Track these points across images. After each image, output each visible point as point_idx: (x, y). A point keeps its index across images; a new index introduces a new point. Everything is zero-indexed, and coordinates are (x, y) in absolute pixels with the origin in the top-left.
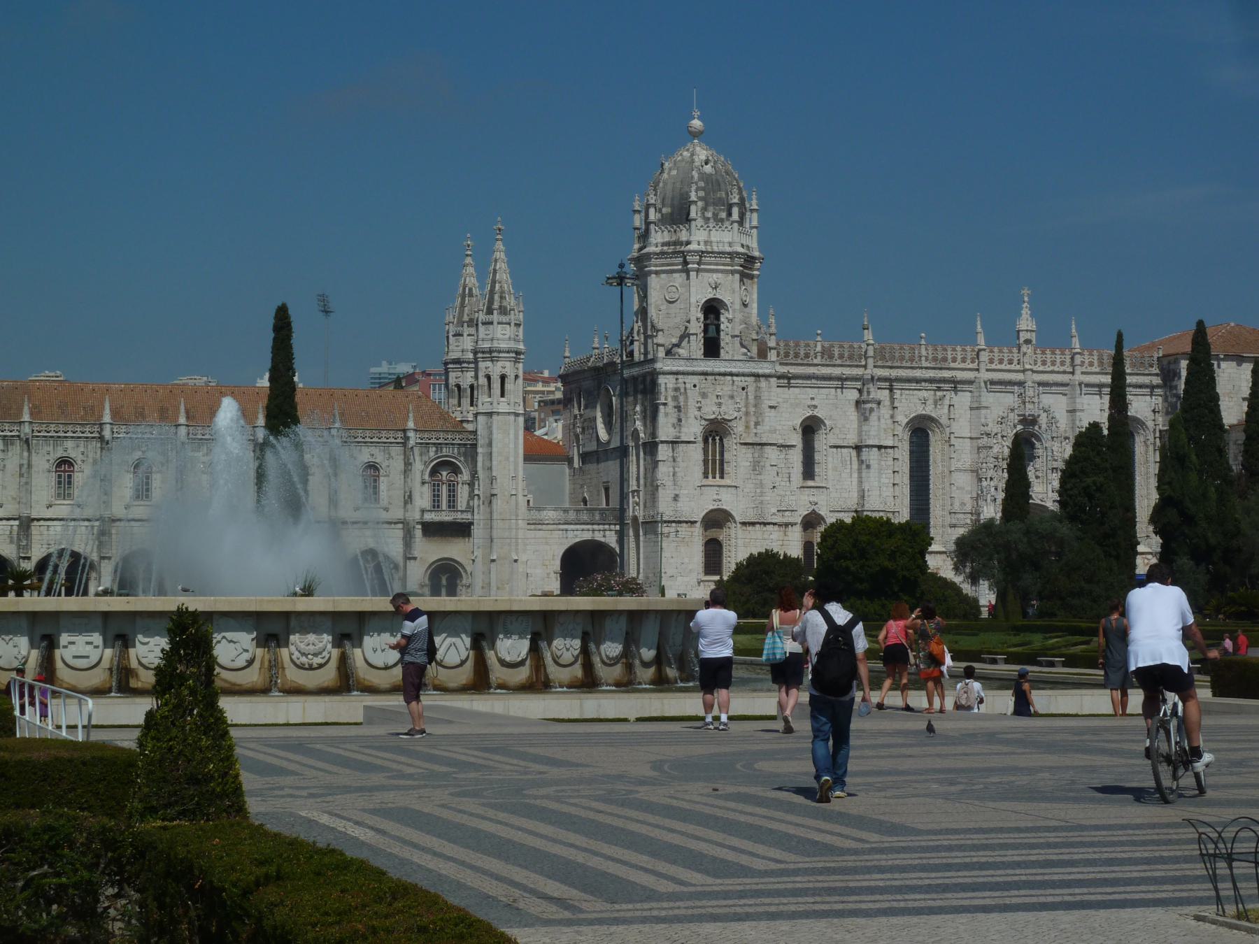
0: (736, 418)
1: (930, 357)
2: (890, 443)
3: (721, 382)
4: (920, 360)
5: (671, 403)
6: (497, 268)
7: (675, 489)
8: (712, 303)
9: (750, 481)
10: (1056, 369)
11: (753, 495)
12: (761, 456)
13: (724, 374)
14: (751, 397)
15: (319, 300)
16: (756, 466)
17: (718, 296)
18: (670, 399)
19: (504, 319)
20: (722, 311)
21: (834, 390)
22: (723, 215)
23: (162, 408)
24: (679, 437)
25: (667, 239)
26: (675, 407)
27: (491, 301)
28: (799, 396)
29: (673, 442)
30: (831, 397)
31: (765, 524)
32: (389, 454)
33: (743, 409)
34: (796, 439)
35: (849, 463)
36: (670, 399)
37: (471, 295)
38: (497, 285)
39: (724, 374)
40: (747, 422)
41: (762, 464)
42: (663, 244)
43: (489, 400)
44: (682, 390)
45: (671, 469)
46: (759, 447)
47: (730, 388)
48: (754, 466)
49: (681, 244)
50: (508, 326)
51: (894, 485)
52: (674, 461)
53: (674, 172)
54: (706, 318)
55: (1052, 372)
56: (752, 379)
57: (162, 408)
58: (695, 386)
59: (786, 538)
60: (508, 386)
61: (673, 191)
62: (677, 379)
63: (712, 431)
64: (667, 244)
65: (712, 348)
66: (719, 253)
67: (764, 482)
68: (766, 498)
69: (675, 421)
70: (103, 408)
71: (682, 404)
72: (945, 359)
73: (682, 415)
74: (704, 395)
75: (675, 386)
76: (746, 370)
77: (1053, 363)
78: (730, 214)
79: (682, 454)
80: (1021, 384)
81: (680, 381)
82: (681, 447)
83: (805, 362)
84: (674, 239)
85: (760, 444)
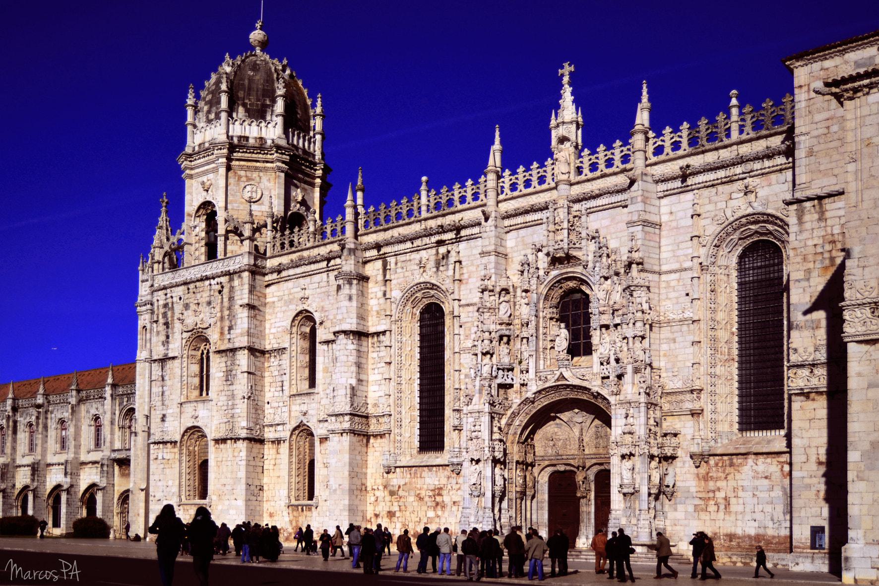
3: (201, 289)
5: (161, 321)
9: (223, 393)
11: (225, 408)
12: (233, 364)
16: (229, 377)
18: (160, 317)
28: (292, 291)
30: (322, 284)
31: (236, 439)
33: (219, 315)
36: (160, 317)
40: (222, 328)
41: (234, 372)
48: (227, 376)
52: (163, 380)
58: (180, 299)
59: (278, 456)
62: (166, 294)
67: (235, 392)
69: (163, 338)
75: (165, 302)
79: (168, 372)
81: (169, 296)
82: (169, 364)
83: (299, 248)
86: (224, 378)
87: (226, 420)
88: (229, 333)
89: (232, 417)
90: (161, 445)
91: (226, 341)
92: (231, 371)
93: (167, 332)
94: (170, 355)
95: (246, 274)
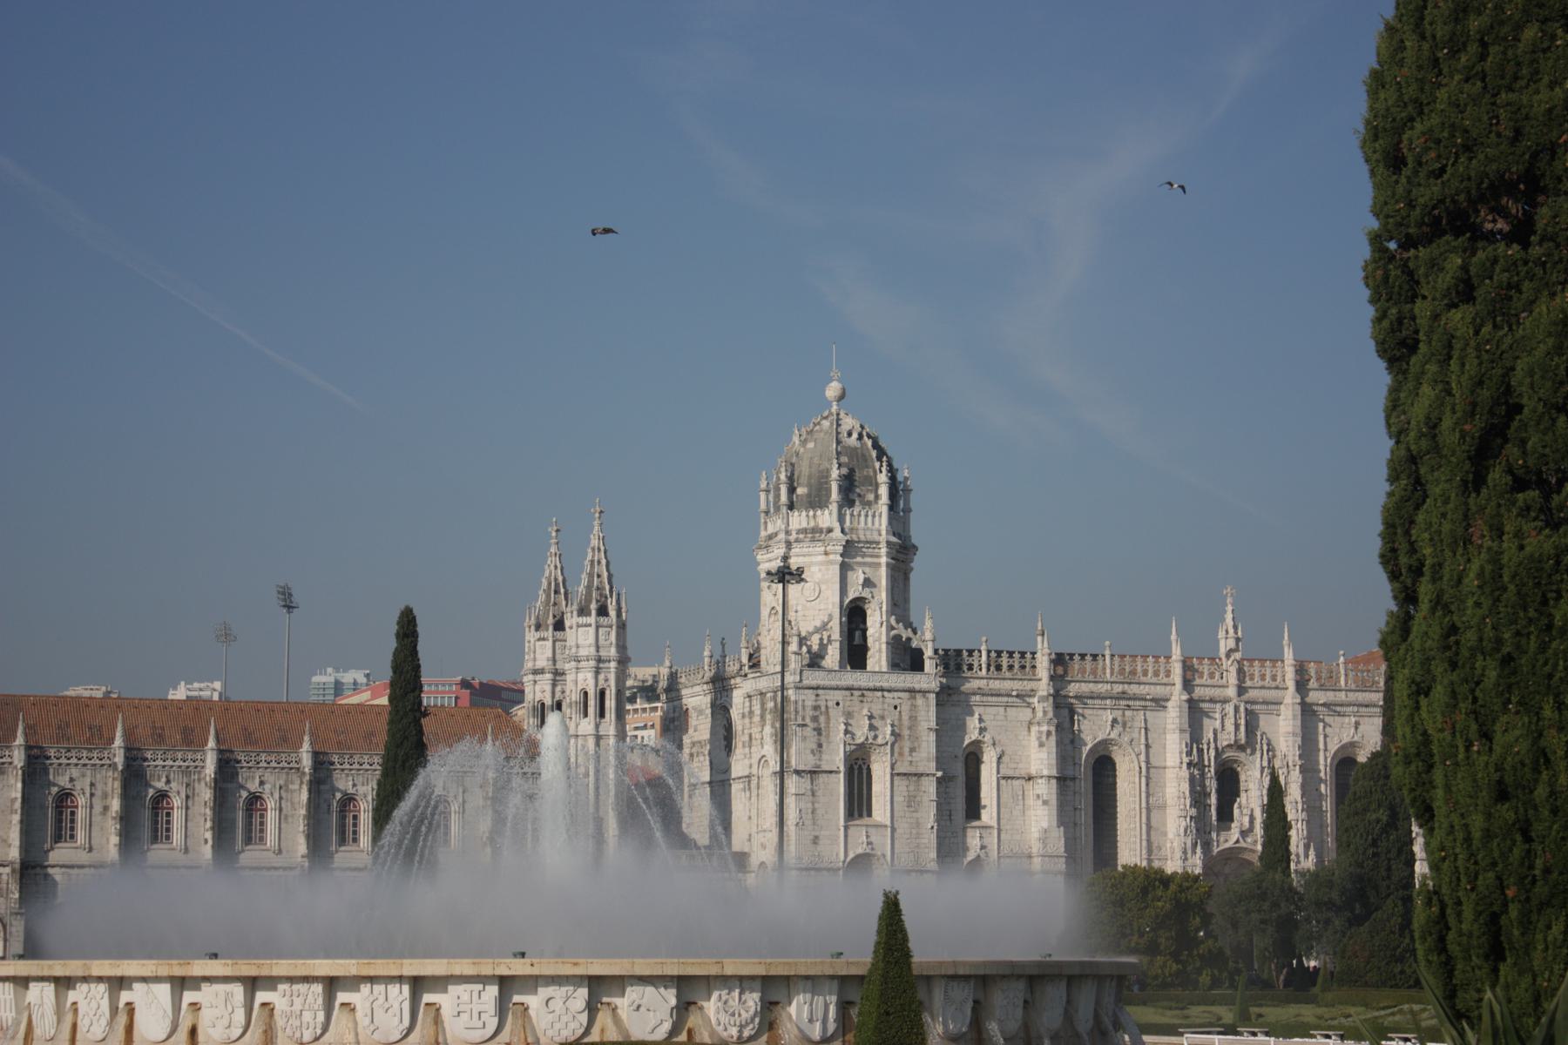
0: (887, 743)
1: (1116, 668)
2: (1070, 773)
3: (869, 700)
4: (1105, 674)
6: (596, 558)
7: (814, 830)
8: (858, 603)
10: (1266, 683)
11: (906, 836)
13: (875, 690)
14: (905, 717)
15: (279, 592)
16: (912, 802)
17: (863, 595)
19: (602, 620)
20: (869, 612)
21: (1002, 709)
22: (871, 497)
23: (185, 728)
24: (819, 767)
25: (804, 525)
26: (815, 729)
27: (588, 600)
29: (814, 773)
30: (999, 718)
31: (922, 872)
32: (463, 785)
34: (959, 769)
35: (1020, 797)
36: (808, 721)
37: (557, 592)
38: (595, 578)
39: (875, 690)
41: (918, 799)
42: (799, 532)
43: (587, 719)
44: (823, 709)
45: (810, 805)
46: (915, 778)
47: (880, 707)
48: (909, 802)
49: (821, 531)
50: (609, 629)
51: (1075, 824)
52: (813, 795)
53: (811, 445)
54: (850, 621)
55: (1263, 687)
56: (905, 695)
57: (185, 728)
58: (838, 704)
60: (610, 703)
61: (810, 467)
63: (857, 759)
64: (804, 531)
65: (856, 655)
66: (867, 542)
68: (923, 841)
69: (814, 746)
70: (115, 728)
71: (823, 725)
72: (1133, 673)
73: (823, 739)
74: (849, 715)
75: (814, 703)
76: (901, 685)
77: (1263, 677)
78: (877, 497)
80: (1225, 701)
81: (822, 697)
82: (822, 778)
84: (812, 524)
85: (915, 775)
86: (905, 804)
87: (908, 850)
88: (911, 755)
89: (918, 846)
90: (813, 873)
91: (907, 764)
92: (915, 797)
93: (819, 740)
94: (825, 767)
95: (932, 696)
